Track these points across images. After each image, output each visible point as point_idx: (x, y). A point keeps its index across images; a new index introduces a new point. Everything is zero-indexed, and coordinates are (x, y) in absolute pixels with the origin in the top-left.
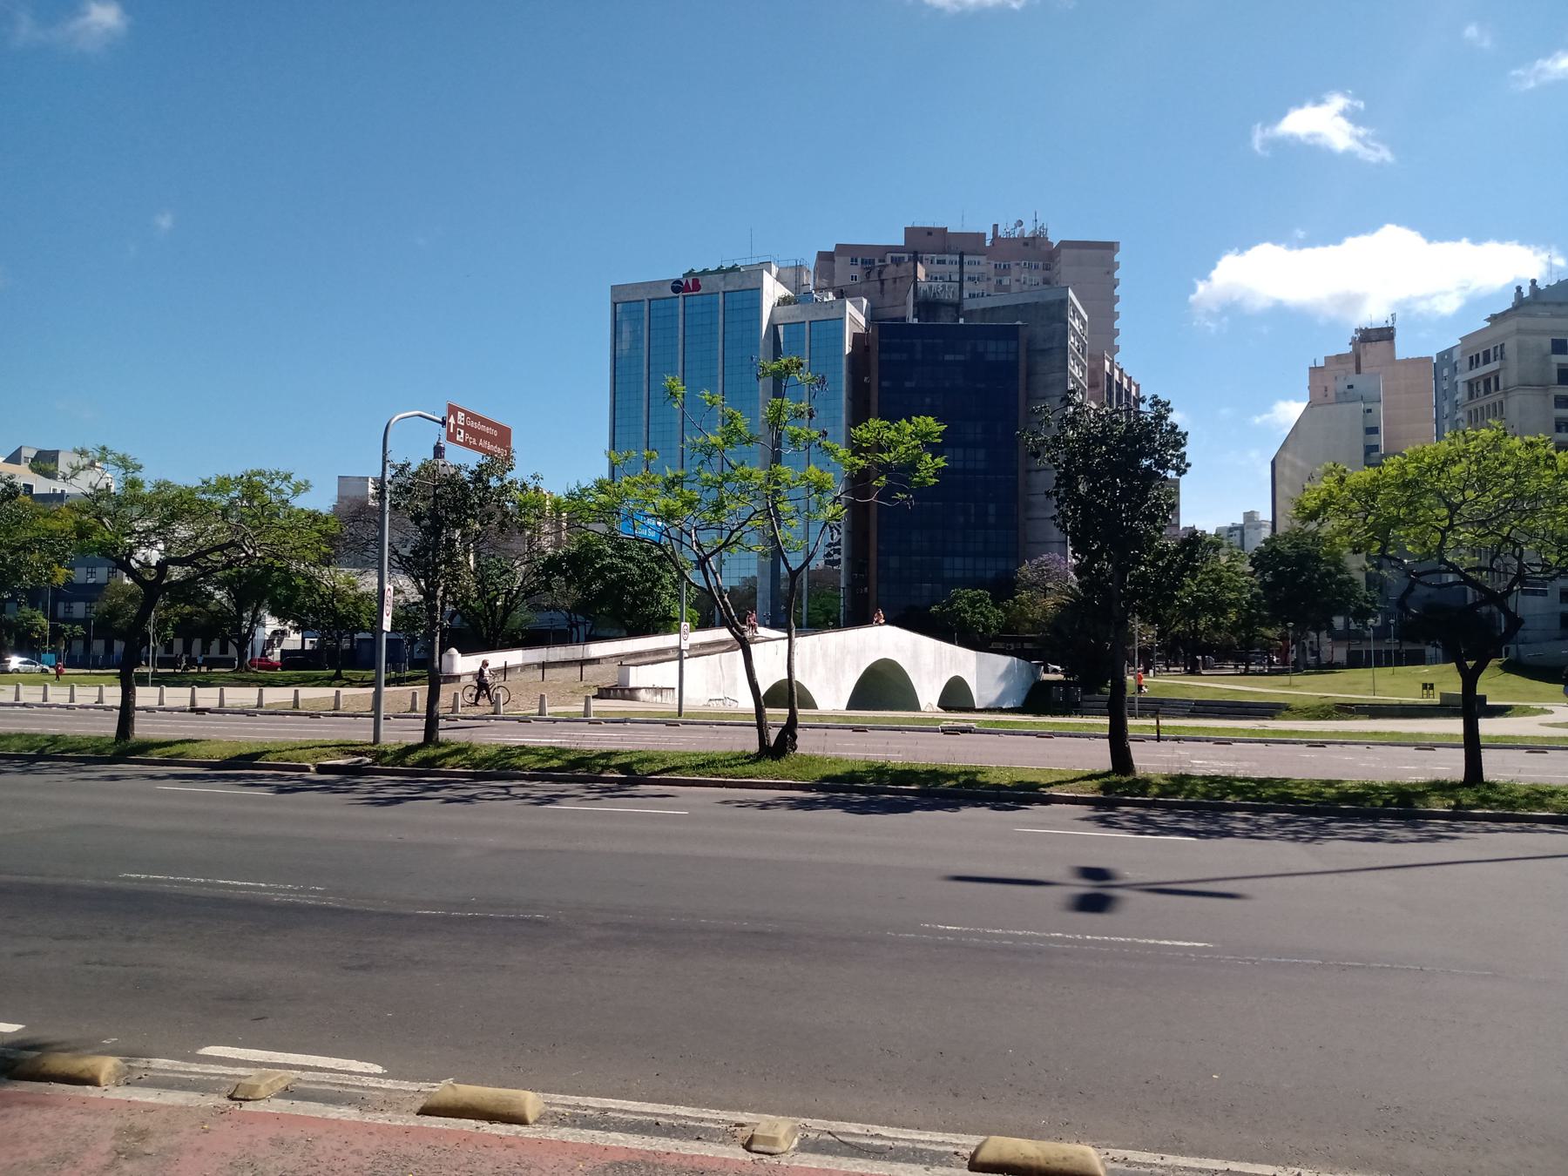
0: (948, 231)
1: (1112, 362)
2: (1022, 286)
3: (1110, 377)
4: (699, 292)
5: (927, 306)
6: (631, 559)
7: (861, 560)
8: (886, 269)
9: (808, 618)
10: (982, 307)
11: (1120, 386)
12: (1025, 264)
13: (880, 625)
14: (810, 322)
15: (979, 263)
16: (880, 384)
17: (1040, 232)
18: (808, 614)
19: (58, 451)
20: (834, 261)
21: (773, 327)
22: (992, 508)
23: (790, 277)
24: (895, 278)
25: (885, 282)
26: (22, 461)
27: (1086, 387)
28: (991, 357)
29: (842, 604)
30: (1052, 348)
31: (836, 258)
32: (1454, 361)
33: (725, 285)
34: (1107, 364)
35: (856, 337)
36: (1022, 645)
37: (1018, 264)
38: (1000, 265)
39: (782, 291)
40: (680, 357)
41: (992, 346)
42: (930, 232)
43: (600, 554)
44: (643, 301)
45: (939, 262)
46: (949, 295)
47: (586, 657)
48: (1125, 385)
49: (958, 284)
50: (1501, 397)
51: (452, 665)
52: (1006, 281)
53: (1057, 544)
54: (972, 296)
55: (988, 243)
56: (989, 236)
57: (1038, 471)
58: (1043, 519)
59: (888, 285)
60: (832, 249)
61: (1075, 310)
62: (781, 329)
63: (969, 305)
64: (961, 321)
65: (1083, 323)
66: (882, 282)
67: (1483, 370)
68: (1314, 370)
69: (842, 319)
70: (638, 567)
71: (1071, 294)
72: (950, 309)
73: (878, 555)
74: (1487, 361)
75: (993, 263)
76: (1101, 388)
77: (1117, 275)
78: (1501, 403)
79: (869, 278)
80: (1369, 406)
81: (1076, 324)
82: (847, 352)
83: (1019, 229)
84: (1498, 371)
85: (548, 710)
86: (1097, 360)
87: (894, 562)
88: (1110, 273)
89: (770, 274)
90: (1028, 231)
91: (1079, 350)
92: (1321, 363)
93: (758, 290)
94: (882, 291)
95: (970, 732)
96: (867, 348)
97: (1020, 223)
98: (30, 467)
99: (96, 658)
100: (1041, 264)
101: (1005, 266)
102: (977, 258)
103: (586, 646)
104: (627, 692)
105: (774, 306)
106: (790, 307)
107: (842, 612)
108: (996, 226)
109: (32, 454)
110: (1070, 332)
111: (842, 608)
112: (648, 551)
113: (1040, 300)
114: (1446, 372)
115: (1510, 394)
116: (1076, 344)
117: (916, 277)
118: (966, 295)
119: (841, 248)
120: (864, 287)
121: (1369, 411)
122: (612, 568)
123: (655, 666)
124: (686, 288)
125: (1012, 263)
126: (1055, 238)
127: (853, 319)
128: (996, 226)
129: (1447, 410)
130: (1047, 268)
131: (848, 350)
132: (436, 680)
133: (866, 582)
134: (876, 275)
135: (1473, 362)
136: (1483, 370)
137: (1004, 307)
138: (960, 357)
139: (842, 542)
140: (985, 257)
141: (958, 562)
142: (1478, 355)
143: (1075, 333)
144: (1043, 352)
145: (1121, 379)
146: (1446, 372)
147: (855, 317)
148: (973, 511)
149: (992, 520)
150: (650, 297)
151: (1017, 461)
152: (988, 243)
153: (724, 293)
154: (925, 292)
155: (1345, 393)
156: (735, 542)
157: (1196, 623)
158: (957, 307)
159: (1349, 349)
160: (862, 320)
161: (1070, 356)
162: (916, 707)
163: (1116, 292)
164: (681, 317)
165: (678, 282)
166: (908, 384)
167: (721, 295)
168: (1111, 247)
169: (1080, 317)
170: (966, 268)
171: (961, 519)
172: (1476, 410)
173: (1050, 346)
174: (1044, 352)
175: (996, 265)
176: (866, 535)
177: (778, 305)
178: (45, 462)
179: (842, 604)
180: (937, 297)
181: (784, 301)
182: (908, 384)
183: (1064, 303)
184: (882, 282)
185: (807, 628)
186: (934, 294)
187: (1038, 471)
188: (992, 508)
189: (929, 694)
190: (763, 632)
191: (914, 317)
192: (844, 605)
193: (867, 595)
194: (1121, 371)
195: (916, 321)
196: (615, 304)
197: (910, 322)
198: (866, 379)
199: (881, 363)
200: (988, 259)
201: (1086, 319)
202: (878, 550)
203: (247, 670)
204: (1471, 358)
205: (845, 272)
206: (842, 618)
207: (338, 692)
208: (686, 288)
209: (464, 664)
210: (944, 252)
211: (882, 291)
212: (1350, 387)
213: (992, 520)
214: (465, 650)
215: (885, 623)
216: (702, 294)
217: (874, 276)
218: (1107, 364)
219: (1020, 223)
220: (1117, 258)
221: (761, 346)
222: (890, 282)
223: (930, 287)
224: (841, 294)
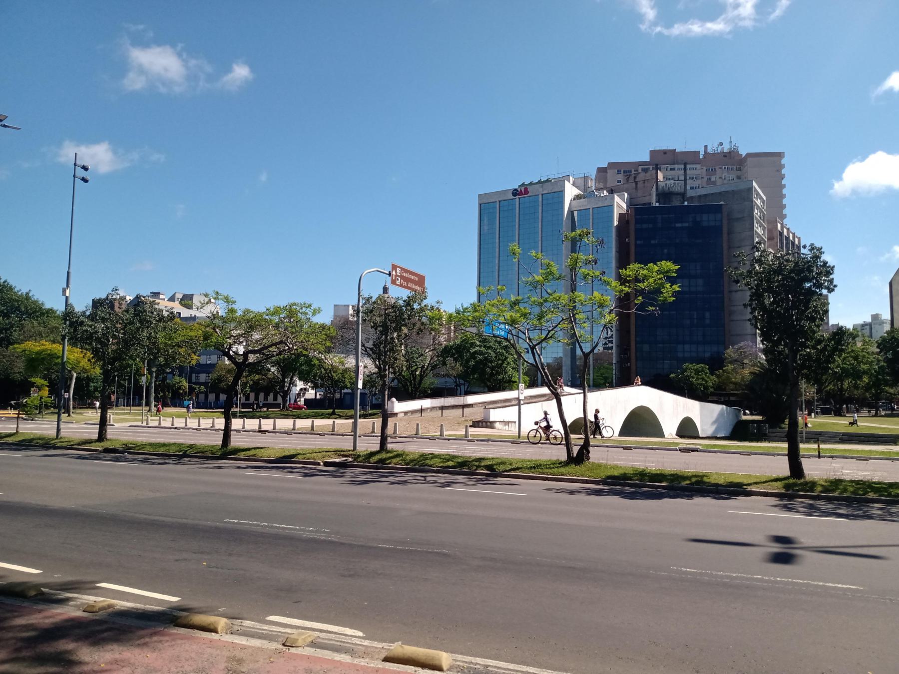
0: (677, 151)
1: (782, 225)
2: (724, 181)
3: (781, 234)
4: (528, 195)
5: (665, 195)
6: (490, 347)
7: (625, 347)
8: (639, 175)
9: (593, 381)
10: (698, 194)
11: (787, 238)
12: (725, 168)
13: (638, 385)
14: (593, 208)
15: (696, 168)
16: (635, 242)
17: (734, 149)
18: (593, 379)
19: (193, 295)
20: (607, 173)
21: (571, 212)
22: (707, 315)
23: (582, 183)
24: (644, 180)
25: (638, 182)
26: (176, 300)
27: (766, 240)
28: (705, 224)
29: (614, 373)
30: (743, 217)
31: (608, 171)
33: (543, 191)
34: (779, 225)
35: (621, 216)
36: (729, 398)
37: (721, 168)
38: (709, 169)
39: (576, 192)
40: (517, 233)
41: (705, 217)
42: (665, 152)
43: (473, 345)
44: (496, 202)
45: (671, 169)
46: (678, 189)
47: (465, 403)
48: (791, 238)
49: (683, 182)
51: (393, 408)
52: (713, 179)
53: (750, 336)
54: (692, 188)
55: (701, 157)
56: (702, 153)
57: (736, 291)
59: (640, 185)
60: (606, 165)
61: (758, 194)
62: (575, 213)
63: (690, 193)
64: (686, 203)
65: (763, 202)
66: (636, 183)
69: (612, 206)
70: (494, 352)
71: (754, 184)
72: (679, 196)
73: (636, 344)
75: (705, 168)
76: (775, 240)
77: (783, 172)
79: (628, 181)
81: (758, 202)
82: (615, 225)
83: (720, 147)
85: (445, 433)
86: (772, 223)
87: (646, 347)
88: (779, 171)
89: (569, 182)
90: (726, 148)
91: (760, 218)
93: (562, 192)
94: (636, 188)
95: (697, 451)
96: (628, 222)
97: (721, 144)
98: (179, 303)
99: (210, 403)
100: (735, 168)
101: (712, 170)
102: (694, 166)
103: (465, 397)
104: (488, 424)
105: (571, 200)
106: (581, 200)
107: (614, 378)
108: (706, 147)
109: (180, 296)
110: (755, 207)
111: (614, 376)
112: (500, 343)
113: (735, 189)
116: (759, 214)
117: (657, 179)
118: (688, 188)
119: (612, 165)
120: (626, 186)
122: (481, 353)
123: (504, 409)
124: (521, 193)
125: (717, 168)
126: (743, 152)
127: (619, 206)
128: (706, 147)
130: (739, 169)
131: (616, 223)
132: (386, 416)
133: (629, 360)
134: (633, 179)
137: (712, 194)
138: (686, 225)
139: (614, 336)
140: (700, 165)
141: (687, 347)
143: (758, 208)
144: (738, 219)
145: (788, 234)
147: (620, 204)
148: (695, 317)
149: (708, 322)
150: (500, 200)
151: (723, 286)
152: (701, 157)
153: (542, 194)
154: (663, 187)
156: (551, 337)
157: (842, 384)
158: (683, 195)
160: (625, 206)
161: (755, 222)
162: (660, 434)
163: (784, 182)
164: (517, 209)
165: (516, 190)
166: (653, 242)
167: (540, 196)
168: (780, 155)
169: (761, 198)
170: (688, 172)
171: (688, 322)
174: (738, 219)
175: (707, 170)
176: (628, 332)
177: (574, 200)
178: (187, 301)
179: (614, 373)
180: (671, 190)
181: (577, 197)
182: (653, 242)
183: (750, 189)
184: (636, 183)
185: (593, 387)
186: (669, 188)
187: (736, 291)
188: (707, 315)
189: (670, 428)
190: (567, 389)
191: (656, 202)
193: (629, 368)
194: (788, 230)
195: (657, 204)
196: (481, 205)
197: (654, 205)
198: (627, 240)
199: (636, 230)
200: (702, 166)
201: (765, 198)
202: (636, 341)
203: (287, 410)
205: (614, 178)
206: (614, 381)
207: (334, 422)
208: (521, 193)
209: (399, 407)
210: (674, 164)
211: (636, 188)
213: (708, 322)
214: (400, 399)
215: (642, 385)
216: (529, 196)
217: (631, 179)
218: (779, 225)
219: (721, 144)
220: (783, 161)
221: (564, 223)
222: (642, 182)
223: (666, 184)
224: (611, 191)
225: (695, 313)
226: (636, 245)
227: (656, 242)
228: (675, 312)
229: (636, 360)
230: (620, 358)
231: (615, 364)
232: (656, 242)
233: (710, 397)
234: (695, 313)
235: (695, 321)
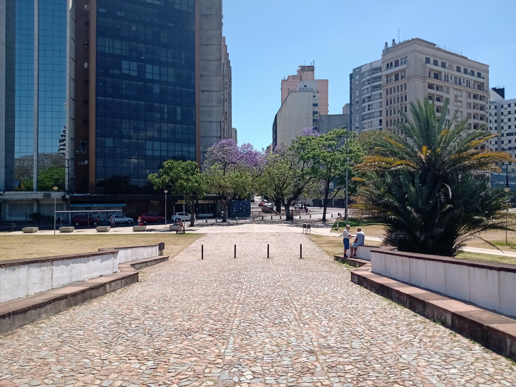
7: (81, 141)
22: (179, 110)
29: (67, 172)
30: (211, 15)
32: (362, 72)
36: (197, 201)
50: (405, 82)
58: (209, 122)
67: (394, 69)
68: (283, 81)
74: (397, 65)
78: (405, 85)
80: (315, 94)
84: (405, 69)
87: (109, 142)
92: (286, 78)
107: (67, 179)
114: (357, 77)
115: (410, 81)
121: (314, 96)
129: (357, 94)
133: (86, 157)
135: (389, 66)
136: (394, 69)
141: (157, 144)
142: (391, 63)
146: (357, 77)
148: (166, 111)
149: (179, 118)
151: (195, 80)
155: (303, 89)
159: (296, 74)
166: (118, 14)
171: (158, 116)
172: (402, 86)
173: (210, 13)
176: (86, 122)
179: (67, 172)
185: (38, 190)
192: (69, 174)
193: (87, 166)
198: (86, 6)
204: (388, 65)
206: (67, 183)
212: (305, 86)
213: (179, 118)
225: (166, 106)
226: (98, 14)
227: (123, 15)
228: (144, 103)
229: (96, 157)
230: (76, 155)
231: (68, 160)
232: (123, 15)
233: (178, 201)
234: (166, 106)
235: (166, 115)
